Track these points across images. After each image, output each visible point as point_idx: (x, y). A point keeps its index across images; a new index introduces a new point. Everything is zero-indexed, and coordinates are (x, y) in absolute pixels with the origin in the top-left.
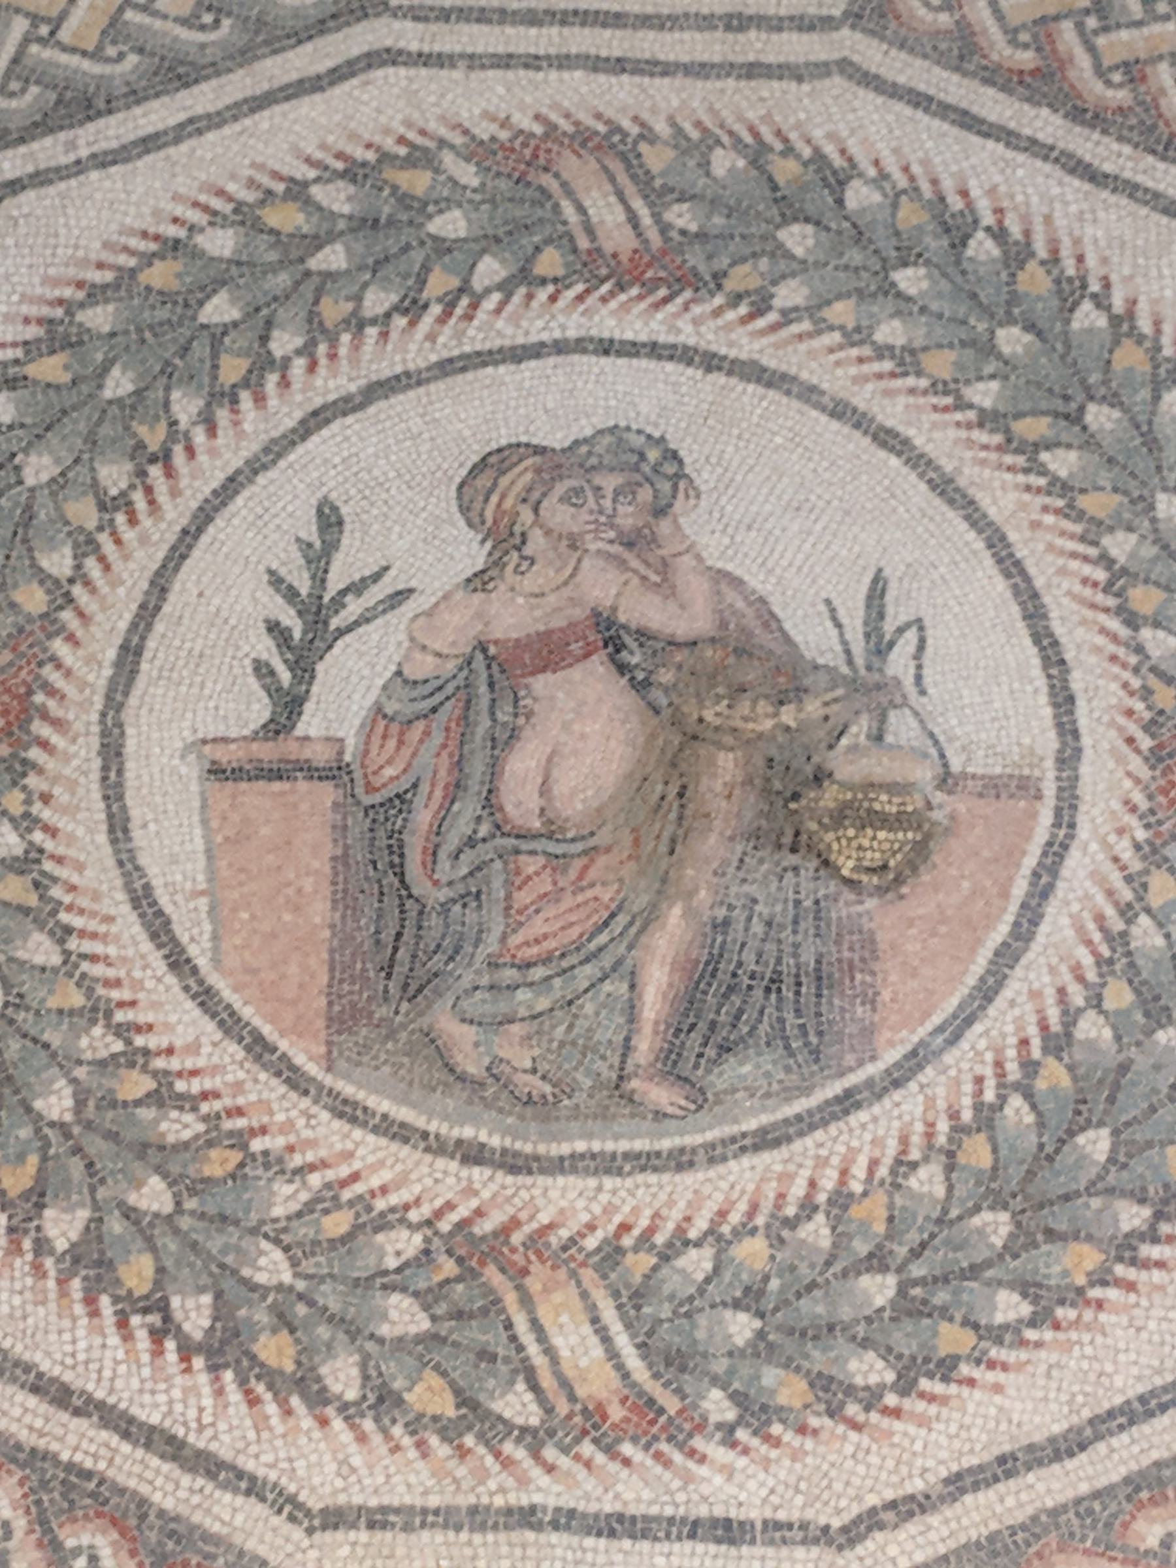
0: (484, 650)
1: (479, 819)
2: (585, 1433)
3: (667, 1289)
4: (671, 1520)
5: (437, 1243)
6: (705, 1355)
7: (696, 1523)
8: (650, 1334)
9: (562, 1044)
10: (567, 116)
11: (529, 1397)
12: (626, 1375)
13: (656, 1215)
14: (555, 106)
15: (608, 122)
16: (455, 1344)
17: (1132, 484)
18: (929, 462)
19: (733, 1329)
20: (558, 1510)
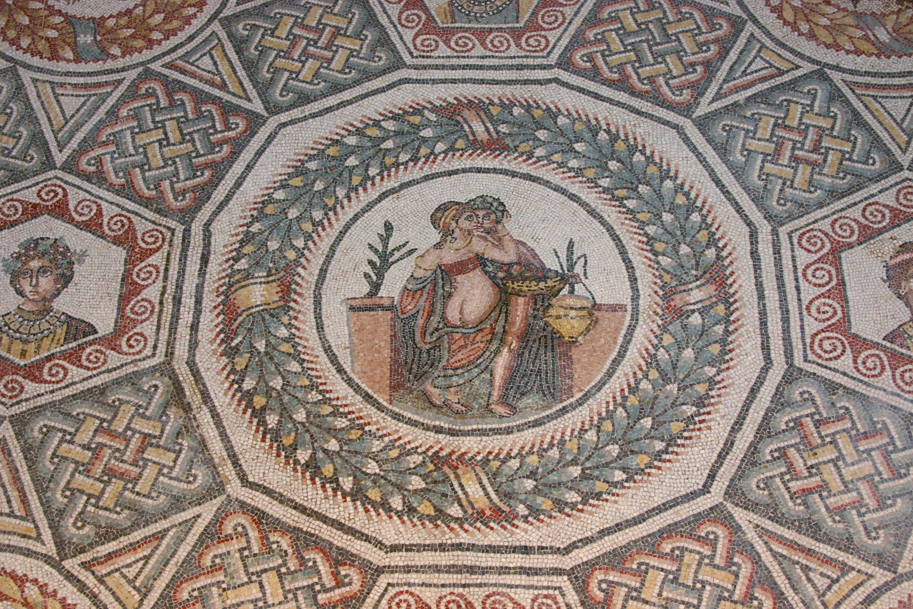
0: (440, 268)
1: (439, 322)
2: (478, 519)
3: (504, 473)
4: (507, 547)
5: (427, 459)
6: (517, 494)
7: (515, 548)
8: (499, 487)
9: (468, 394)
10: (465, 98)
11: (459, 508)
12: (491, 501)
13: (501, 449)
14: (461, 95)
15: (479, 99)
16: (434, 492)
17: (654, 210)
18: (587, 205)
19: (527, 485)
20: (469, 544)
